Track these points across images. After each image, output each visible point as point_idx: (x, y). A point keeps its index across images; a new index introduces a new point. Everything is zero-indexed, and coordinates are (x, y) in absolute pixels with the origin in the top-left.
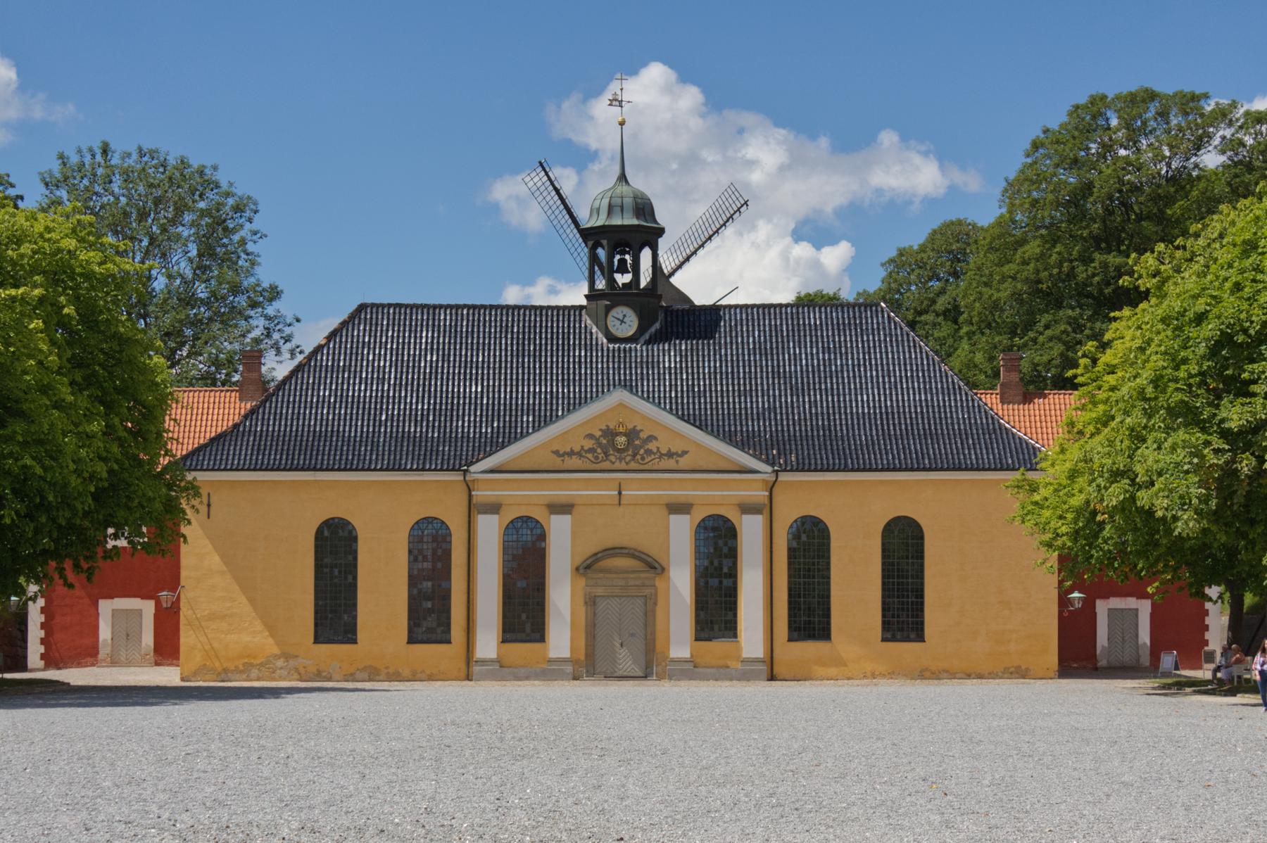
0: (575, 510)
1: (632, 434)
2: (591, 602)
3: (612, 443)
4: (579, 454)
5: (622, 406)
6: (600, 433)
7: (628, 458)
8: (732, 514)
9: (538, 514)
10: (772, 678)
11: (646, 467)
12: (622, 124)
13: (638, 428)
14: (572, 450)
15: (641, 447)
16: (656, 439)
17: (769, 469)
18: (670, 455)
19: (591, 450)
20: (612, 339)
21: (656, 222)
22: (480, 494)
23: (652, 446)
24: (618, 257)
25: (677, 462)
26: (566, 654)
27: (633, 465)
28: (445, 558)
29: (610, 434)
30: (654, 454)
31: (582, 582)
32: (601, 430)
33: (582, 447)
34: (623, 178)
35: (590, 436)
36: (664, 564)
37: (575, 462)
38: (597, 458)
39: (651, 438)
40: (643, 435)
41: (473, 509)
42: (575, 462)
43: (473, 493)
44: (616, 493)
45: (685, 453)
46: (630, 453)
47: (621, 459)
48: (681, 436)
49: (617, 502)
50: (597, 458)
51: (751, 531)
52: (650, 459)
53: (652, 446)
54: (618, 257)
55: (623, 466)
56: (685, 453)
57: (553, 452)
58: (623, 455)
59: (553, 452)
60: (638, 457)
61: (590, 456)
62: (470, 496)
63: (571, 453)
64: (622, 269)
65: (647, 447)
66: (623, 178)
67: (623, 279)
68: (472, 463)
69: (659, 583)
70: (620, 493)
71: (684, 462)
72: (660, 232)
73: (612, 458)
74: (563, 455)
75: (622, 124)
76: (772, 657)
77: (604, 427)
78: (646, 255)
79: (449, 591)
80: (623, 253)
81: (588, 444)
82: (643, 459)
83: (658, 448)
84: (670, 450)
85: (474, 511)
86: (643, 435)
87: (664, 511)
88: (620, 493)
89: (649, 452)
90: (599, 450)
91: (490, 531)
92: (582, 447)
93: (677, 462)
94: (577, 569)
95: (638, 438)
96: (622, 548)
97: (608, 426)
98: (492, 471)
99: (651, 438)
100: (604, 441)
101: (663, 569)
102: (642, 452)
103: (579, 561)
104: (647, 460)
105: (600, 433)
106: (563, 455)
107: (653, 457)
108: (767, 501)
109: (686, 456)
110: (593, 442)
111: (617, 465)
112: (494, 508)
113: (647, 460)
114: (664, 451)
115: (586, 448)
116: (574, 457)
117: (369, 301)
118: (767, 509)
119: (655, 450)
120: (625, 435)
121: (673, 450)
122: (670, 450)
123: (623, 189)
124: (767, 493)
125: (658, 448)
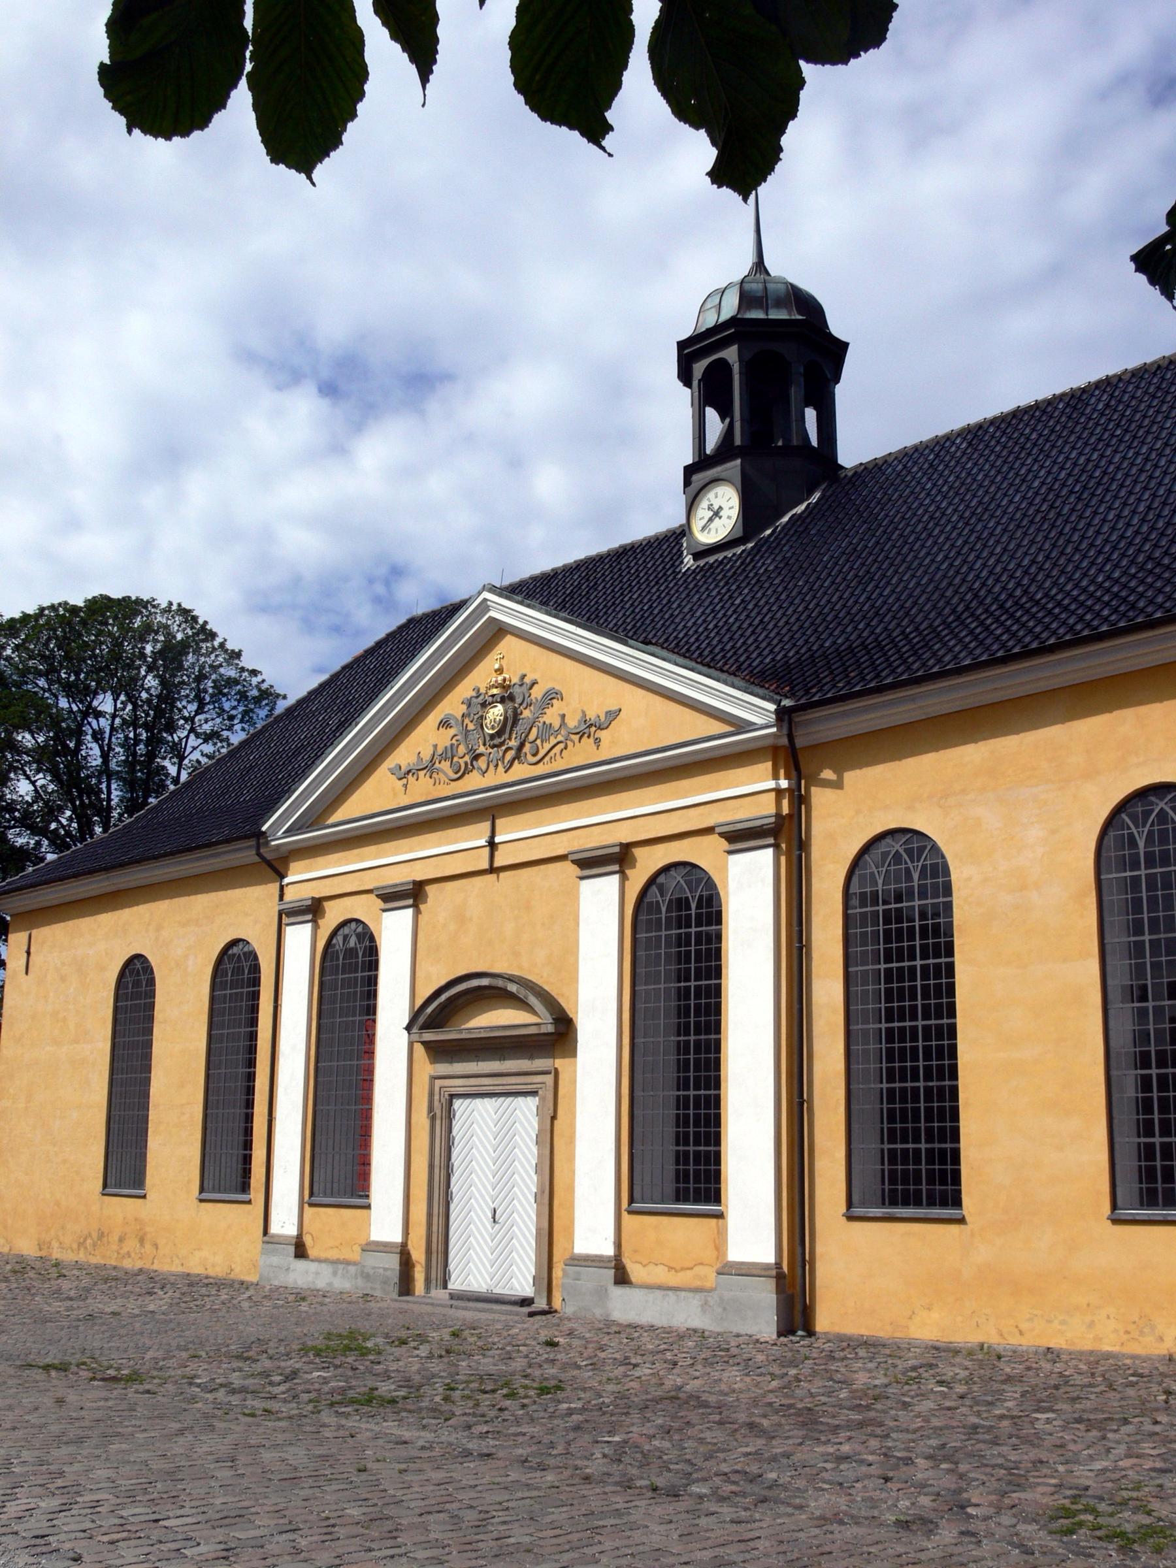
9: (363, 909)
25: (597, 741)
27: (520, 771)
34: (760, 264)
39: (552, 696)
44: (482, 842)
45: (613, 715)
52: (547, 746)
53: (551, 716)
56: (613, 715)
66: (760, 264)
70: (492, 845)
86: (537, 693)
99: (552, 696)
104: (542, 753)
113: (542, 753)
114: (572, 723)
119: (556, 724)
120: (502, 701)
121: (591, 715)
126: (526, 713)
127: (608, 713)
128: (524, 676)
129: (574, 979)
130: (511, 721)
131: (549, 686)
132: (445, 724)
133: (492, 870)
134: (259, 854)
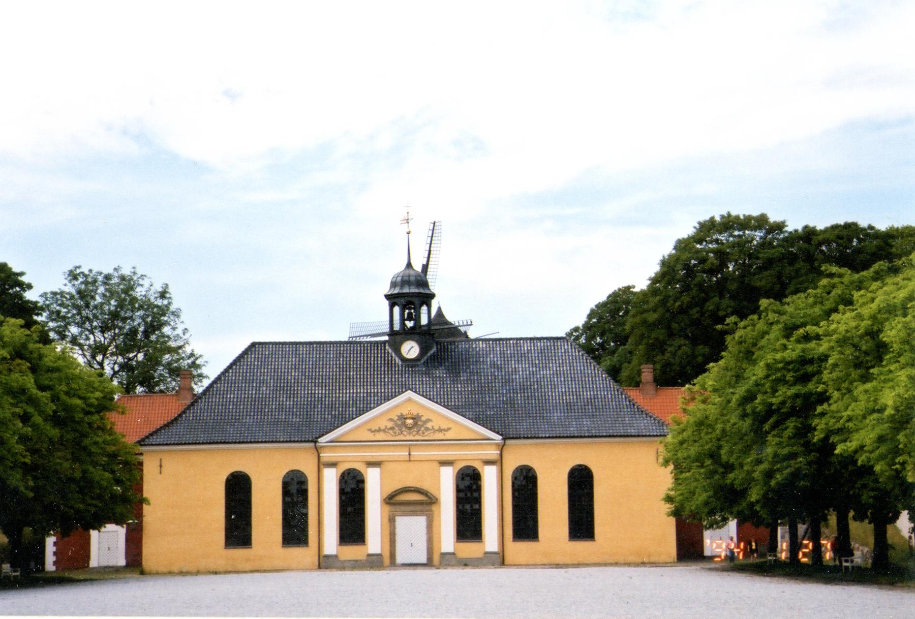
0: (383, 466)
1: (416, 418)
2: (392, 521)
3: (404, 424)
4: (384, 431)
5: (409, 400)
7: (414, 433)
8: (477, 465)
9: (360, 467)
10: (503, 563)
12: (408, 233)
13: (420, 415)
14: (380, 428)
15: (422, 426)
17: (500, 437)
18: (440, 430)
19: (392, 428)
20: (404, 360)
21: (429, 289)
22: (326, 456)
23: (429, 425)
24: (407, 311)
25: (445, 434)
26: (378, 551)
27: (417, 438)
28: (304, 493)
29: (403, 418)
31: (387, 508)
32: (397, 416)
33: (386, 426)
34: (409, 265)
35: (391, 420)
36: (437, 497)
37: (380, 436)
39: (429, 420)
40: (423, 419)
41: (321, 465)
42: (380, 436)
43: (321, 455)
44: (407, 454)
45: (449, 429)
46: (415, 430)
47: (410, 434)
48: (448, 418)
51: (489, 478)
53: (429, 425)
54: (407, 311)
55: (411, 438)
56: (449, 429)
57: (369, 430)
58: (411, 431)
59: (369, 430)
60: (421, 432)
61: (391, 431)
62: (319, 457)
63: (379, 430)
64: (410, 318)
65: (425, 426)
66: (409, 265)
67: (409, 324)
68: (320, 437)
69: (434, 508)
70: (410, 454)
71: (449, 435)
72: (432, 296)
73: (405, 433)
75: (408, 233)
76: (503, 551)
77: (399, 414)
78: (424, 309)
79: (306, 515)
80: (410, 309)
81: (390, 425)
82: (423, 433)
83: (433, 427)
85: (322, 466)
86: (423, 419)
87: (436, 465)
88: (410, 454)
89: (427, 429)
90: (396, 428)
91: (331, 481)
92: (386, 426)
93: (445, 434)
94: (385, 500)
95: (421, 421)
96: (410, 487)
97: (402, 414)
98: (331, 442)
99: (429, 420)
101: (437, 499)
102: (423, 429)
103: (385, 496)
107: (429, 432)
108: (499, 457)
109: (450, 431)
110: (393, 423)
111: (408, 438)
112: (333, 465)
113: (426, 434)
114: (436, 428)
115: (388, 427)
117: (257, 340)
118: (498, 462)
119: (431, 428)
120: (413, 418)
123: (411, 272)
124: (499, 452)
125: (433, 427)
126: (419, 423)
129: (439, 489)
130: (415, 424)
132: (391, 420)
133: (410, 461)
134: (315, 445)
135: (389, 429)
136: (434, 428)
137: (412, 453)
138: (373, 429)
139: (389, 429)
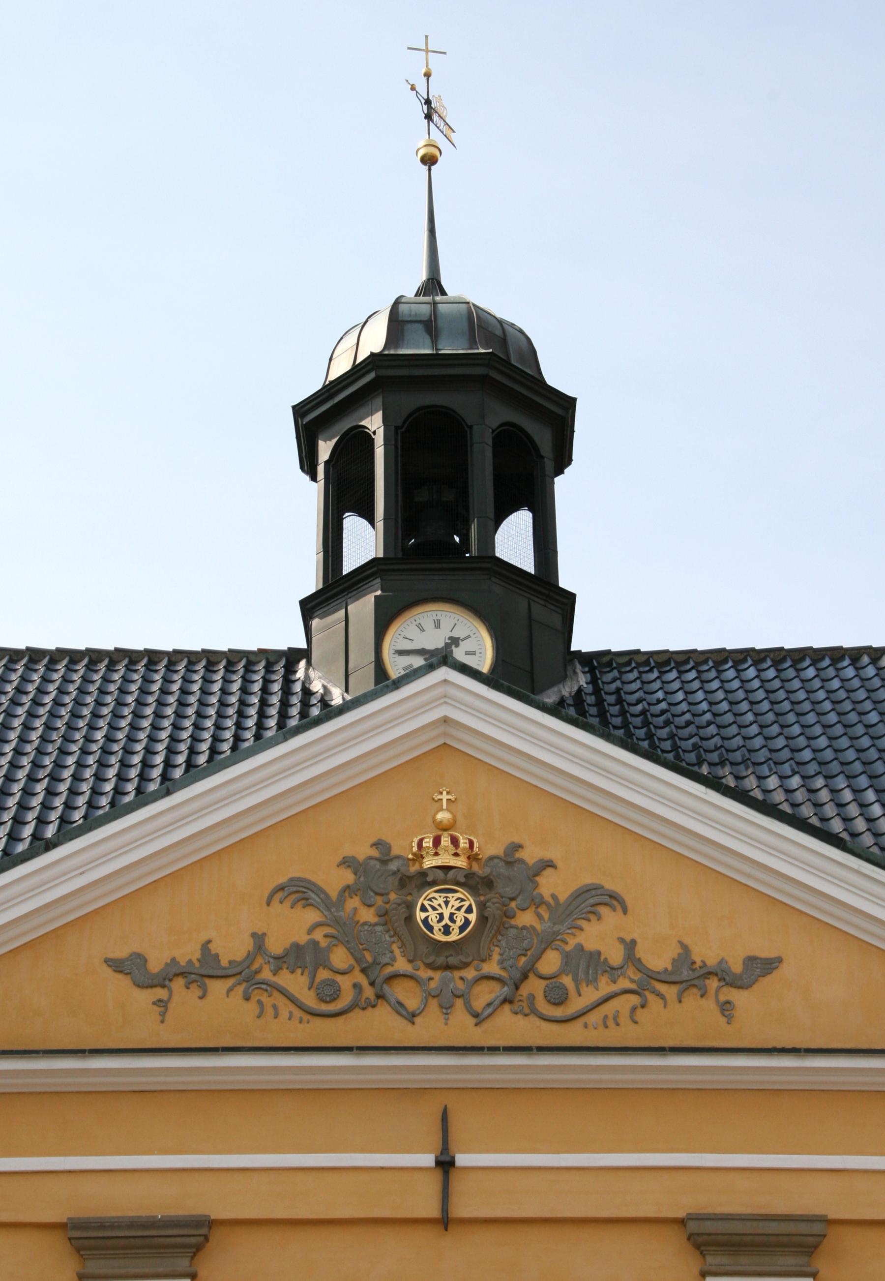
6: (348, 877)
7: (484, 995)
11: (573, 1034)
13: (530, 855)
15: (549, 942)
16: (614, 900)
25: (726, 1008)
30: (613, 972)
32: (347, 862)
33: (259, 939)
38: (329, 991)
44: (428, 1160)
46: (492, 967)
49: (432, 1210)
50: (329, 991)
52: (590, 995)
57: (117, 966)
59: (117, 966)
60: (534, 987)
70: (445, 1165)
74: (162, 980)
77: (363, 851)
82: (558, 997)
83: (630, 946)
84: (685, 955)
88: (445, 1165)
90: (340, 957)
92: (259, 939)
93: (726, 1008)
95: (538, 902)
100: (367, 915)
102: (550, 962)
104: (575, 1005)
105: (348, 877)
106: (162, 980)
107: (605, 987)
110: (312, 916)
113: (575, 1005)
115: (276, 945)
116: (217, 988)
119: (615, 955)
122: (685, 955)
127: (750, 961)
128: (518, 847)
131: (587, 879)
135: (280, 961)
136: (641, 952)
137: (462, 1160)
138: (155, 965)
139: (280, 961)
